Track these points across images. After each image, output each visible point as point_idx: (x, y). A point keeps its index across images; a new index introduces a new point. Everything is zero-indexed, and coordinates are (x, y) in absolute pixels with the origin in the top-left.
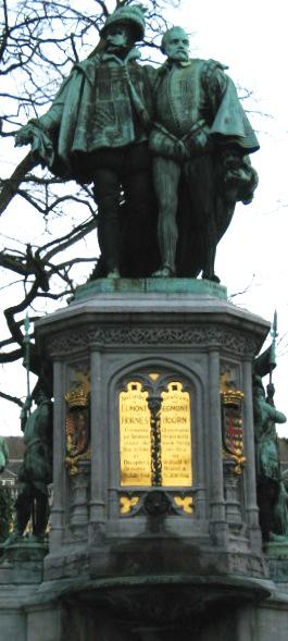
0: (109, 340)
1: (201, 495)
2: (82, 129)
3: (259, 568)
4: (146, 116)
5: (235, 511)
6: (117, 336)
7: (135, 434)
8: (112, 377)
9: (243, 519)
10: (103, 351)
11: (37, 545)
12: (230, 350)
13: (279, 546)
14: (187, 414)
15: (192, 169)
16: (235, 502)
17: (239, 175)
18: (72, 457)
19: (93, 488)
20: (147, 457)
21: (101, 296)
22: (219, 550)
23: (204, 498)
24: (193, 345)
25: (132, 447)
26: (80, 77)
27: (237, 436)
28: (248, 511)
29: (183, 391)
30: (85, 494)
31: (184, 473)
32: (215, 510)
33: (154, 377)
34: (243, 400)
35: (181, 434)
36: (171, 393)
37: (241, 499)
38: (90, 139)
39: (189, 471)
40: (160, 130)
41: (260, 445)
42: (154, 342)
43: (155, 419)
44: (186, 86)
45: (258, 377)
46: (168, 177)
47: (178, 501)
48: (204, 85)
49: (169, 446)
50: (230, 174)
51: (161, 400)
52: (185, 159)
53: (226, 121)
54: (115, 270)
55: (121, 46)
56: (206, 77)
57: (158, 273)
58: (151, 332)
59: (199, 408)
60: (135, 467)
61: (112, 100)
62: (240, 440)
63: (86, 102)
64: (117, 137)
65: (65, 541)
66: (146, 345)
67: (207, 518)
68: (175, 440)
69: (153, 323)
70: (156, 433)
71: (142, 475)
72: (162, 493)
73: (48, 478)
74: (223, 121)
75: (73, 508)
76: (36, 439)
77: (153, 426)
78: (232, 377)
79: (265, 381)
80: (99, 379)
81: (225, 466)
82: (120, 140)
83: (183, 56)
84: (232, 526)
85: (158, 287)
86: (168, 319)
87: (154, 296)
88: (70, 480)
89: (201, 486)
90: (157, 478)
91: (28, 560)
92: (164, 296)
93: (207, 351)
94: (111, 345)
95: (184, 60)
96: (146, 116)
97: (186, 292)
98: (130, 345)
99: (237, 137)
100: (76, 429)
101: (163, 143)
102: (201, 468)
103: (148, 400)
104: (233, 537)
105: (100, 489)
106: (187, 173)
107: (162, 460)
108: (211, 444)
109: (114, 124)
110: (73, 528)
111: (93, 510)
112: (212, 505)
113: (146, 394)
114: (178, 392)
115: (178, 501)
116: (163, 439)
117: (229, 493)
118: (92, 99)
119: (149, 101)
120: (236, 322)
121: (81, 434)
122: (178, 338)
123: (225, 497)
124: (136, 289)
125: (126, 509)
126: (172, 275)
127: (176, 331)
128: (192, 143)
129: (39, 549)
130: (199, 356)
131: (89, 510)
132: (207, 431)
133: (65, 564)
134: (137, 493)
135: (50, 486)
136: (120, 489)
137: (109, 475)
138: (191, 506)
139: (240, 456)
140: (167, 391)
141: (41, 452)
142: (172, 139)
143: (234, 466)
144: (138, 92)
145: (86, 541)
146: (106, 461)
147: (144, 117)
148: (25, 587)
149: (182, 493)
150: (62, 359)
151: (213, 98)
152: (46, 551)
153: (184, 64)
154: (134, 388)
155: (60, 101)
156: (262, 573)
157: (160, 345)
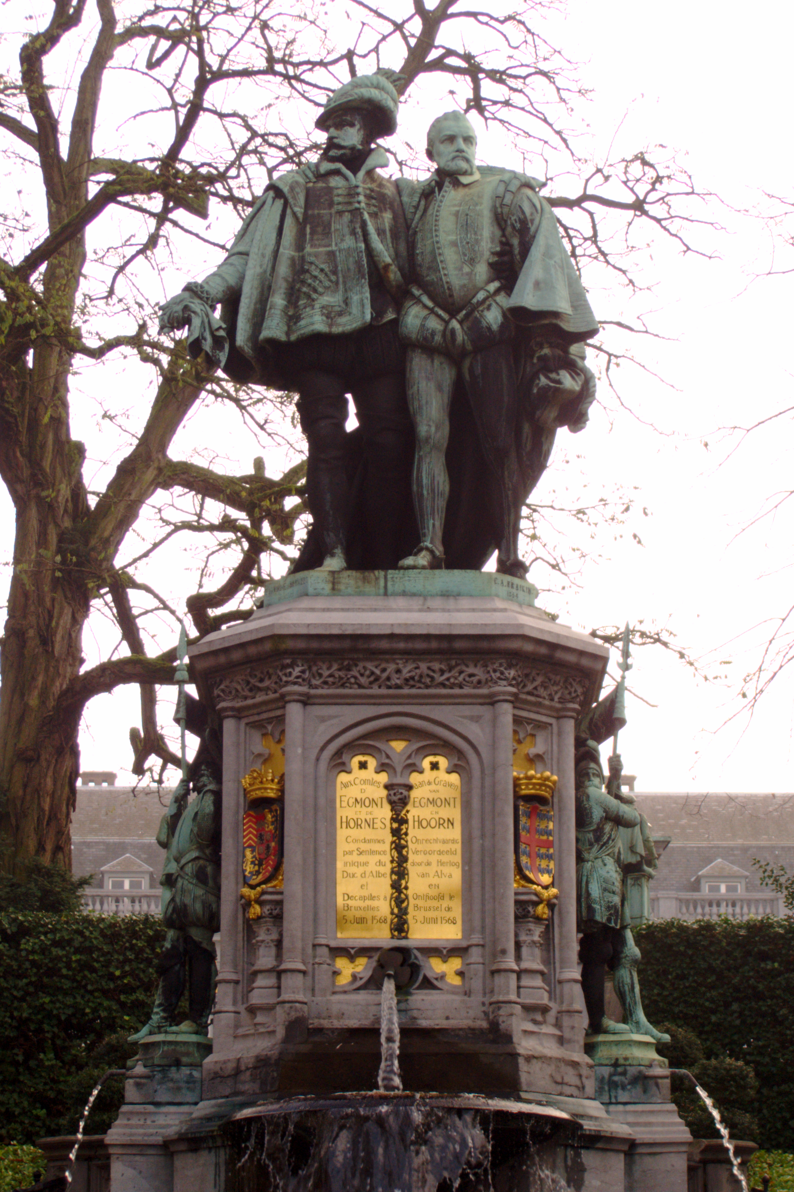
1: (475, 955)
2: (278, 300)
3: (575, 1081)
4: (394, 275)
5: (538, 982)
6: (331, 676)
7: (364, 847)
8: (323, 749)
10: (306, 701)
11: (194, 1038)
12: (530, 698)
13: (618, 1043)
14: (455, 813)
15: (478, 370)
16: (537, 966)
17: (559, 382)
18: (253, 887)
19: (286, 943)
20: (383, 887)
21: (305, 603)
23: (481, 960)
24: (467, 690)
25: (358, 871)
26: (279, 203)
27: (543, 851)
28: (560, 982)
29: (449, 772)
30: (273, 951)
31: (448, 915)
32: (499, 980)
33: (398, 746)
34: (554, 789)
35: (446, 847)
36: (429, 774)
37: (548, 960)
38: (293, 319)
39: (457, 912)
40: (418, 301)
41: (588, 865)
42: (398, 687)
43: (399, 822)
44: (466, 224)
45: (591, 743)
46: (432, 385)
47: (437, 966)
48: (500, 220)
50: (543, 381)
51: (410, 788)
52: (464, 353)
53: (537, 284)
54: (338, 551)
55: (353, 148)
56: (502, 205)
57: (409, 561)
58: (392, 667)
59: (476, 803)
60: (360, 903)
61: (334, 248)
62: (549, 857)
63: (287, 251)
64: (340, 314)
65: (241, 1031)
66: (384, 691)
67: (485, 994)
68: (434, 859)
70: (399, 847)
71: (373, 918)
72: (404, 952)
73: (212, 924)
74: (530, 285)
75: (255, 973)
76: (195, 854)
77: (396, 832)
78: (539, 747)
79: (605, 750)
80: (300, 751)
81: (517, 902)
82: (343, 320)
83: (464, 165)
84: (528, 1009)
86: (420, 645)
87: (401, 602)
88: (250, 927)
89: (476, 939)
90: (400, 926)
91: (178, 1064)
92: (416, 603)
93: (492, 701)
94: (320, 691)
95: (465, 173)
96: (394, 275)
97: (458, 595)
100: (260, 837)
101: (423, 326)
102: (477, 907)
103: (387, 787)
104: (530, 1027)
105: (299, 945)
106: (467, 377)
107: (410, 892)
108: (494, 867)
109: (336, 290)
110: (252, 1010)
111: (288, 981)
112: (493, 973)
113: (383, 778)
114: (442, 775)
115: (437, 966)
116: (411, 857)
117: (525, 951)
118: (299, 246)
119: (402, 247)
120: (543, 650)
121: (268, 847)
123: (518, 958)
124: (368, 588)
125: (344, 980)
126: (435, 564)
127: (436, 666)
128: (475, 328)
129: (198, 1045)
131: (279, 978)
132: (488, 843)
133: (238, 1072)
134: (364, 951)
135: (216, 937)
136: (333, 944)
137: (315, 920)
138: (460, 974)
139: (546, 887)
140: (421, 772)
141: (201, 877)
142: (439, 316)
143: (536, 904)
144: (380, 232)
145: (274, 1032)
146: (311, 894)
147: (392, 276)
148: (172, 1109)
150: (238, 714)
151: (515, 242)
152: (207, 1049)
153: (465, 180)
154: (363, 766)
155: (241, 248)
156: (583, 1088)
157: (406, 691)
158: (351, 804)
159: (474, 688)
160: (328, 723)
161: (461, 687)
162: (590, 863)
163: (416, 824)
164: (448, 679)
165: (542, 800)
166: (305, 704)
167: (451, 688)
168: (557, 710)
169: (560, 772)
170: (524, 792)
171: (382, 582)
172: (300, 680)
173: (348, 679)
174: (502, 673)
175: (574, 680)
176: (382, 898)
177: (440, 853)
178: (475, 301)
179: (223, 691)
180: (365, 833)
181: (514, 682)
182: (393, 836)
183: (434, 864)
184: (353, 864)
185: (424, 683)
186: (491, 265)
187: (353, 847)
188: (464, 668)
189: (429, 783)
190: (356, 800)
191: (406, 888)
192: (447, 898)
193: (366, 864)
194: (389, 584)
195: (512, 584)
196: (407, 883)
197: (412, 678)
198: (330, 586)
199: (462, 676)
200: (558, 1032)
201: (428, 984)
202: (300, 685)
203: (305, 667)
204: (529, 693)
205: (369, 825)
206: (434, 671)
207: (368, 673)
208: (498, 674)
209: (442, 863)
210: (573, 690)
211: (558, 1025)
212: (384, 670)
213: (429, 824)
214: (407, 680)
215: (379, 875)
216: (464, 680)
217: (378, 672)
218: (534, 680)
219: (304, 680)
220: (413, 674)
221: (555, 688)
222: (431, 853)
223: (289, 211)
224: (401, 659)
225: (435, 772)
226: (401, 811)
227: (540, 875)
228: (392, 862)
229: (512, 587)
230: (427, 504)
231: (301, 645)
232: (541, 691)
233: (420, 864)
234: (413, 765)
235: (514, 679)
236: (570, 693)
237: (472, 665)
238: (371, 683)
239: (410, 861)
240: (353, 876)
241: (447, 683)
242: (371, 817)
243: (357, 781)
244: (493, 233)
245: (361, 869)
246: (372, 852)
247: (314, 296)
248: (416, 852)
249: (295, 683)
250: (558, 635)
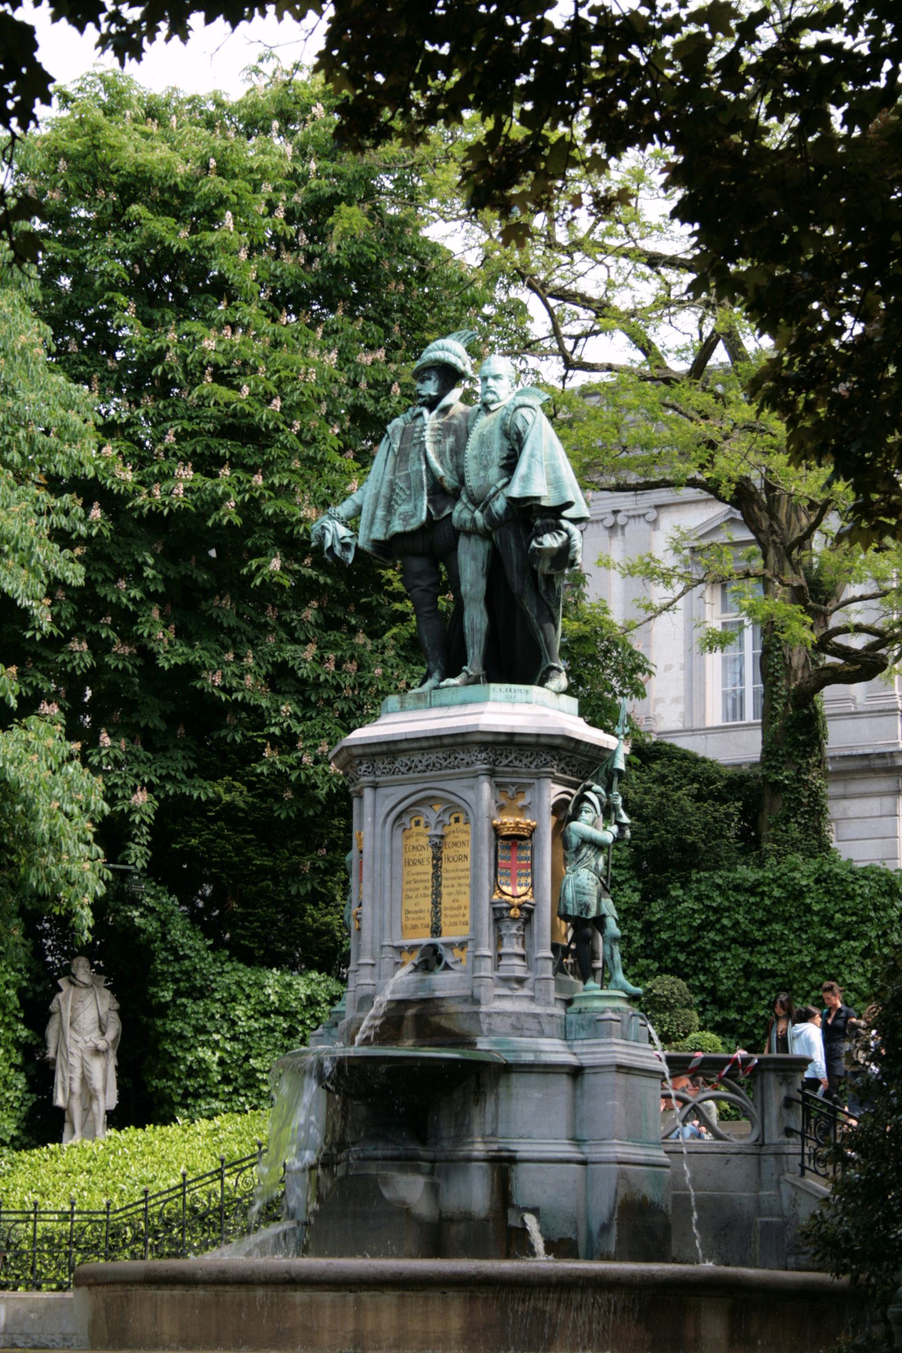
2: (380, 513)
7: (418, 878)
8: (388, 815)
9: (529, 968)
10: (375, 786)
22: (475, 1008)
24: (463, 769)
33: (438, 808)
36: (454, 826)
46: (468, 558)
48: (506, 434)
49: (450, 890)
51: (442, 837)
58: (416, 759)
62: (526, 875)
64: (412, 516)
66: (416, 775)
68: (455, 882)
69: (414, 749)
84: (505, 980)
86: (425, 744)
90: (436, 931)
95: (493, 402)
96: (449, 481)
98: (400, 776)
99: (538, 498)
116: (444, 883)
117: (505, 940)
124: (421, 704)
127: (441, 755)
130: (471, 781)
134: (413, 948)
136: (396, 944)
137: (382, 929)
143: (509, 909)
149: (462, 945)
153: (492, 407)
157: (428, 773)
165: (523, 838)
169: (540, 815)
180: (418, 868)
186: (503, 467)
187: (411, 878)
200: (531, 993)
201: (447, 967)
211: (533, 989)
215: (425, 896)
230: (469, 640)
231: (359, 751)
232: (516, 763)
246: (422, 881)
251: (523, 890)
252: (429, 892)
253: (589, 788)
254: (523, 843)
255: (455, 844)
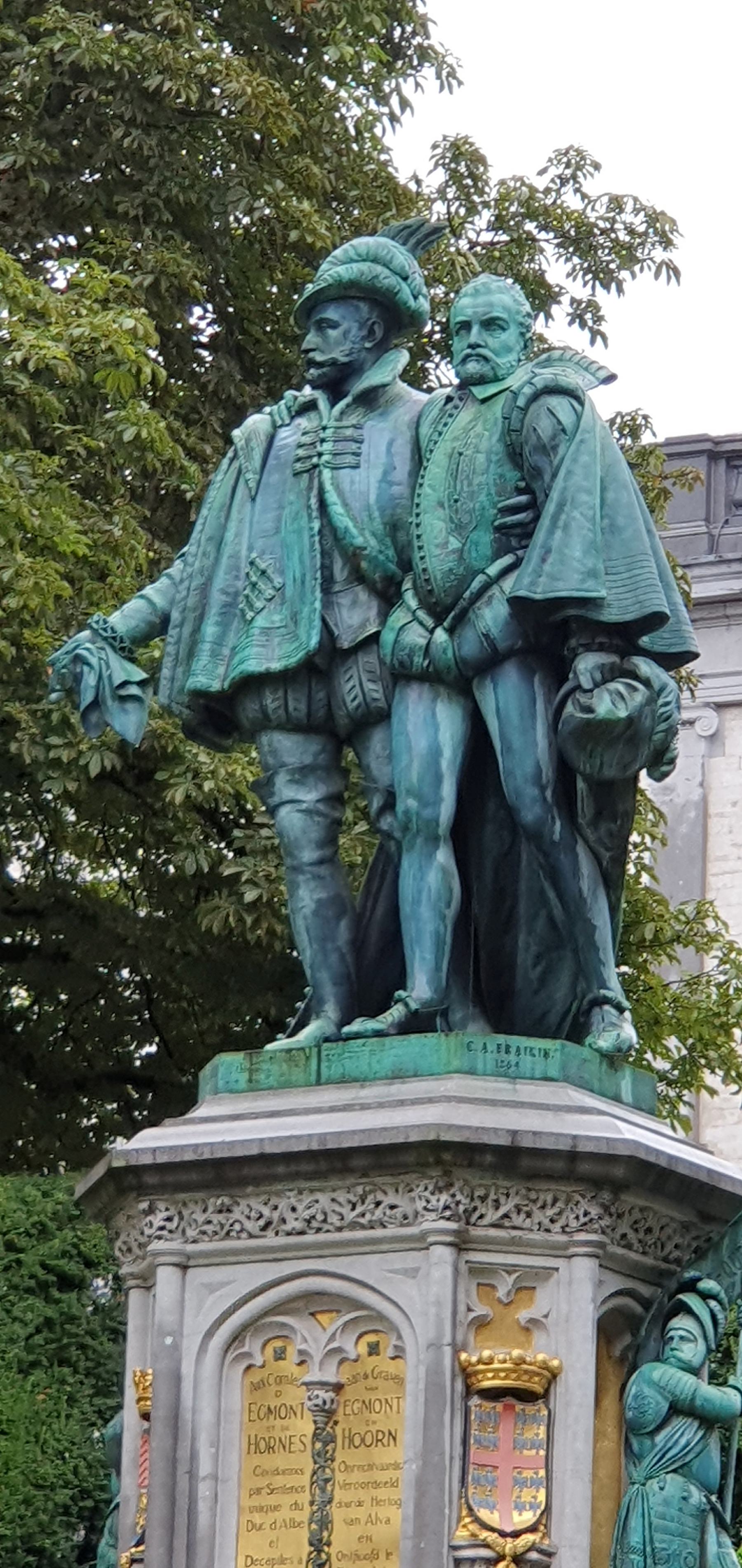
0: (191, 1233)
8: (210, 1334)
24: (391, 1231)
55: (334, 363)
58: (283, 1204)
62: (535, 1484)
66: (282, 1240)
85: (351, 1066)
93: (421, 1243)
107: (333, 1550)
116: (339, 1495)
122: (351, 1216)
127: (342, 1196)
130: (412, 1259)
139: (516, 1535)
157: (309, 1238)
158: (262, 1416)
159: (402, 1225)
160: (218, 1293)
161: (385, 1227)
162: (636, 1486)
163: (347, 1441)
164: (363, 1215)
165: (526, 1396)
166: (184, 1268)
167: (372, 1228)
168: (566, 1246)
170: (487, 1384)
171: (314, 1062)
172: (165, 1233)
173: (231, 1225)
174: (428, 1201)
175: (583, 1197)
176: (296, 1561)
177: (376, 1485)
178: (467, 594)
179: (120, 1249)
180: (279, 1460)
181: (448, 1213)
182: (315, 1463)
183: (367, 1503)
184: (261, 1509)
185: (332, 1224)
188: (380, 1196)
189: (366, 1377)
190: (269, 1408)
191: (329, 1544)
192: (382, 1556)
193: (276, 1508)
194: (324, 1065)
195: (508, 1047)
196: (330, 1536)
197: (313, 1217)
198: (246, 1075)
199: (381, 1207)
202: (167, 1240)
203: (172, 1212)
204: (494, 1226)
205: (284, 1447)
206: (340, 1204)
207: (253, 1214)
208: (424, 1204)
209: (376, 1502)
210: (581, 1213)
212: (276, 1208)
213: (363, 1440)
214: (305, 1220)
216: (385, 1214)
217: (266, 1211)
218: (497, 1205)
219: (171, 1231)
220: (312, 1211)
221: (550, 1212)
222: (364, 1485)
223: (242, 481)
224: (290, 1190)
225: (374, 1358)
226: (326, 1424)
227: (515, 1514)
228: (312, 1503)
229: (507, 1052)
232: (518, 1220)
233: (348, 1505)
234: (339, 1350)
235: (446, 1208)
236: (577, 1218)
237: (391, 1192)
238: (264, 1228)
239: (336, 1500)
240: (260, 1528)
241: (362, 1221)
242: (288, 1433)
243: (271, 1380)
244: (501, 476)
245: (272, 1516)
247: (250, 615)
248: (346, 1486)
249: (159, 1238)
250: (514, 1133)
251: (528, 1517)
252: (304, 1515)
253: (691, 1286)
254: (530, 1409)
255: (368, 1406)
